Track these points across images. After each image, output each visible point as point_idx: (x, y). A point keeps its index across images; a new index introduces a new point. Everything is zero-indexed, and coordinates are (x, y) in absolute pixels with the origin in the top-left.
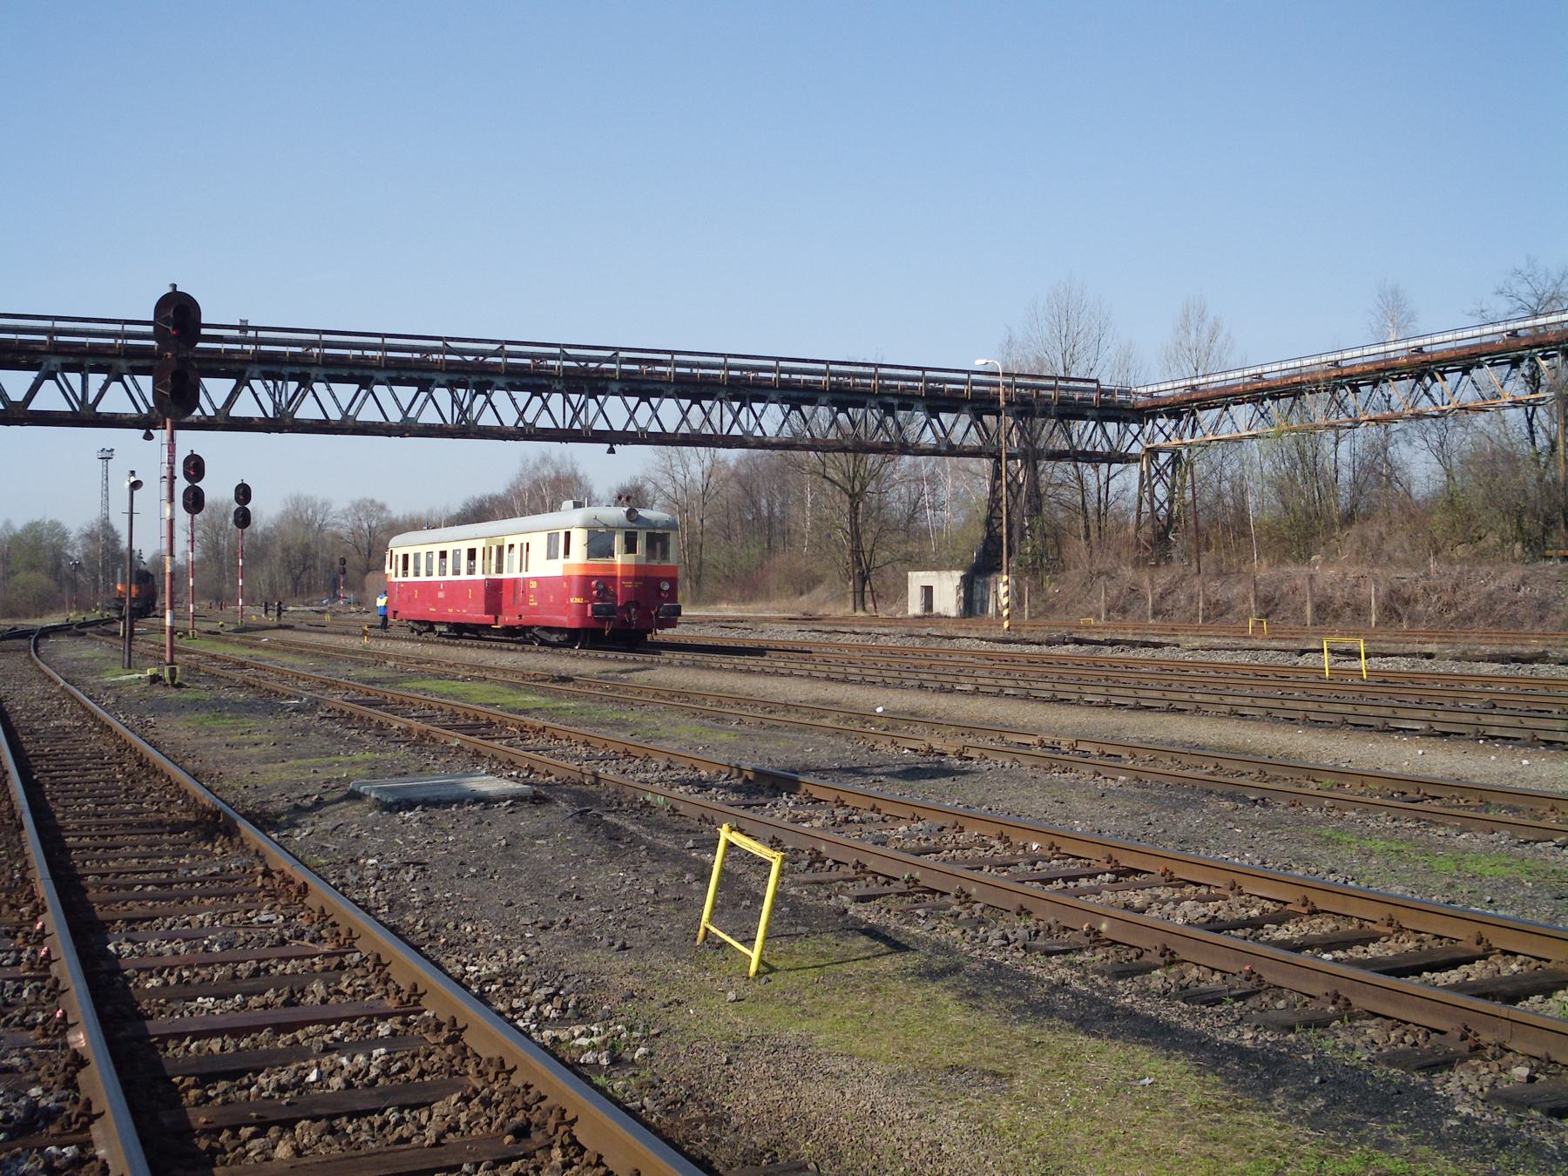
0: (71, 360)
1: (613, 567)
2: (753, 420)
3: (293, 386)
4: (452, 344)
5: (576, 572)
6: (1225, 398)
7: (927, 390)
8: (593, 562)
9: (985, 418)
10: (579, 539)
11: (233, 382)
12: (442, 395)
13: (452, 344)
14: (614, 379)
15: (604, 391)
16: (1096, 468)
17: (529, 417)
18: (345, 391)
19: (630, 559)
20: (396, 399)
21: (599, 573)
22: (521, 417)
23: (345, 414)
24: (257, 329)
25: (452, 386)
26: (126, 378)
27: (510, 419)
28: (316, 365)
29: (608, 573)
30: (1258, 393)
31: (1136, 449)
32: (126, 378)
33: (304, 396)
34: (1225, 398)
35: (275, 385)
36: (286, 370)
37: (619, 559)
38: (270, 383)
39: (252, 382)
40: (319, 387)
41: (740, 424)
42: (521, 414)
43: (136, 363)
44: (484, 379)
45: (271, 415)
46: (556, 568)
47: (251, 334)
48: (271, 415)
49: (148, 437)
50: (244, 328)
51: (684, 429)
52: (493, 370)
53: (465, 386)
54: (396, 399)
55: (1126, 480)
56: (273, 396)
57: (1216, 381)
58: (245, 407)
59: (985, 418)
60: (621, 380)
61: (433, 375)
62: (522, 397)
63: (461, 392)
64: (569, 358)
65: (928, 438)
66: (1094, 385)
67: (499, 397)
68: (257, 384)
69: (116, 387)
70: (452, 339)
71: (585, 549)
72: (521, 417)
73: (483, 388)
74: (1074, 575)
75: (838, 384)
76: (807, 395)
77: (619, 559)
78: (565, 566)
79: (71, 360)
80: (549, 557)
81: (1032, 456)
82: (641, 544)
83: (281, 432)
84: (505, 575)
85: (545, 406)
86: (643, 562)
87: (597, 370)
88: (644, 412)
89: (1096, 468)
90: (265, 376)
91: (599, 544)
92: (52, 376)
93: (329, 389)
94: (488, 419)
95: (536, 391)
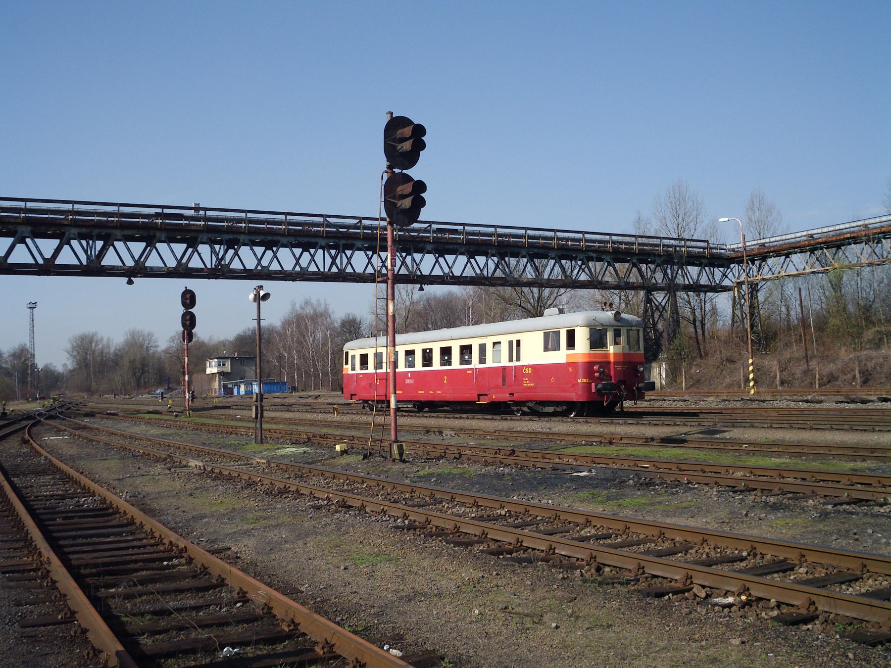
0: (84, 230)
1: (607, 355)
2: (415, 266)
3: (99, 244)
4: (330, 220)
5: (581, 360)
6: (786, 251)
7: (613, 248)
8: (592, 352)
9: (563, 262)
10: (582, 337)
11: (57, 241)
12: (204, 249)
13: (330, 220)
14: (429, 242)
15: (314, 246)
16: (698, 296)
17: (265, 263)
18: (137, 247)
19: (619, 349)
20: (172, 251)
21: (599, 360)
22: (297, 263)
23: (179, 262)
24: (206, 209)
25: (212, 242)
26: (28, 240)
27: (251, 264)
28: (244, 233)
29: (604, 360)
30: (811, 246)
31: (726, 283)
32: (28, 240)
33: (151, 251)
34: (786, 251)
35: (88, 244)
36: (96, 232)
37: (611, 349)
38: (84, 242)
39: (116, 243)
40: (119, 245)
41: (407, 266)
42: (259, 260)
43: (129, 232)
44: (349, 242)
45: (85, 263)
46: (560, 356)
47: (202, 213)
48: (85, 263)
49: (130, 282)
50: (197, 209)
51: (370, 270)
52: (355, 237)
53: (220, 243)
54: (172, 251)
55: (723, 302)
56: (86, 252)
57: (773, 239)
58: (66, 257)
59: (536, 260)
60: (434, 243)
61: (317, 240)
62: (259, 250)
63: (217, 247)
64: (330, 225)
65: (583, 277)
66: (705, 245)
67: (245, 251)
68: (74, 243)
69: (20, 247)
70: (330, 216)
71: (588, 342)
72: (297, 263)
73: (232, 244)
74: (712, 361)
75: (503, 242)
76: (541, 251)
77: (611, 349)
78: (568, 356)
79: (84, 230)
80: (546, 349)
81: (671, 288)
82: (623, 339)
83: (216, 279)
84: (524, 361)
85: (312, 259)
86: (627, 351)
87: (418, 237)
88: (306, 258)
89: (698, 296)
90: (80, 237)
91: (597, 340)
92: (23, 241)
93: (252, 249)
94: (236, 265)
95: (269, 246)
